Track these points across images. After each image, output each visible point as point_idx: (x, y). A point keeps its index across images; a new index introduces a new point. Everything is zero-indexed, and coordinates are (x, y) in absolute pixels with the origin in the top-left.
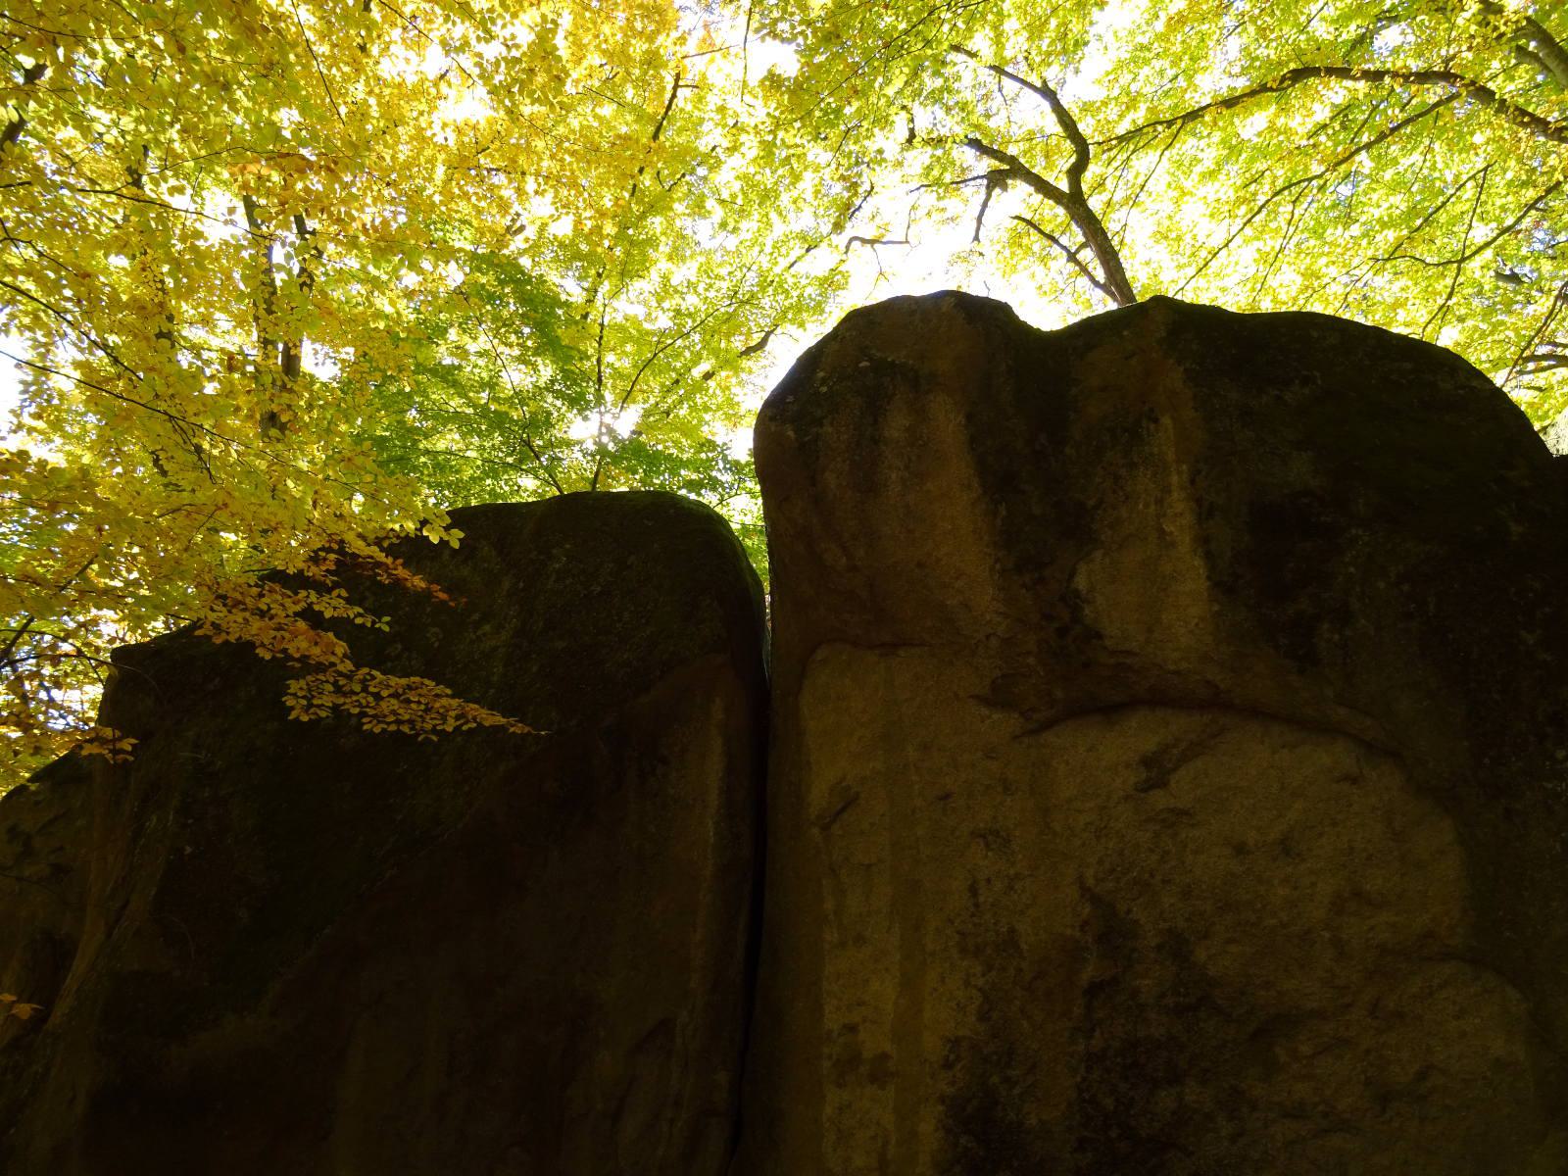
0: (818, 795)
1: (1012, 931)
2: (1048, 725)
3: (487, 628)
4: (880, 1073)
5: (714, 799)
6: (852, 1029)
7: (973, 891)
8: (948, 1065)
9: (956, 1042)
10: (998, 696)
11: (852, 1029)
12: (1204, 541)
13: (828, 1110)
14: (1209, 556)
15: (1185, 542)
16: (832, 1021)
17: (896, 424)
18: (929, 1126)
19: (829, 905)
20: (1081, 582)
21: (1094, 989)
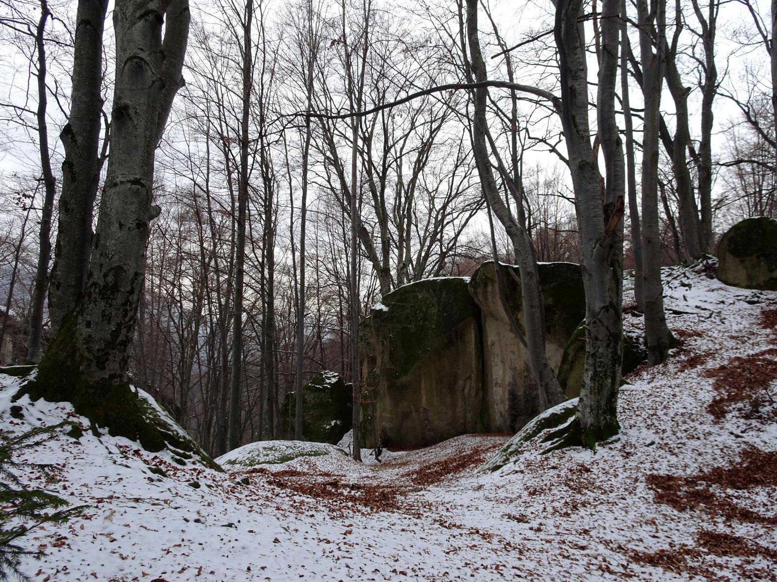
0: (489, 343)
4: (500, 386)
5: (473, 341)
10: (511, 331)
16: (494, 377)
17: (490, 288)
20: (519, 317)
21: (525, 377)
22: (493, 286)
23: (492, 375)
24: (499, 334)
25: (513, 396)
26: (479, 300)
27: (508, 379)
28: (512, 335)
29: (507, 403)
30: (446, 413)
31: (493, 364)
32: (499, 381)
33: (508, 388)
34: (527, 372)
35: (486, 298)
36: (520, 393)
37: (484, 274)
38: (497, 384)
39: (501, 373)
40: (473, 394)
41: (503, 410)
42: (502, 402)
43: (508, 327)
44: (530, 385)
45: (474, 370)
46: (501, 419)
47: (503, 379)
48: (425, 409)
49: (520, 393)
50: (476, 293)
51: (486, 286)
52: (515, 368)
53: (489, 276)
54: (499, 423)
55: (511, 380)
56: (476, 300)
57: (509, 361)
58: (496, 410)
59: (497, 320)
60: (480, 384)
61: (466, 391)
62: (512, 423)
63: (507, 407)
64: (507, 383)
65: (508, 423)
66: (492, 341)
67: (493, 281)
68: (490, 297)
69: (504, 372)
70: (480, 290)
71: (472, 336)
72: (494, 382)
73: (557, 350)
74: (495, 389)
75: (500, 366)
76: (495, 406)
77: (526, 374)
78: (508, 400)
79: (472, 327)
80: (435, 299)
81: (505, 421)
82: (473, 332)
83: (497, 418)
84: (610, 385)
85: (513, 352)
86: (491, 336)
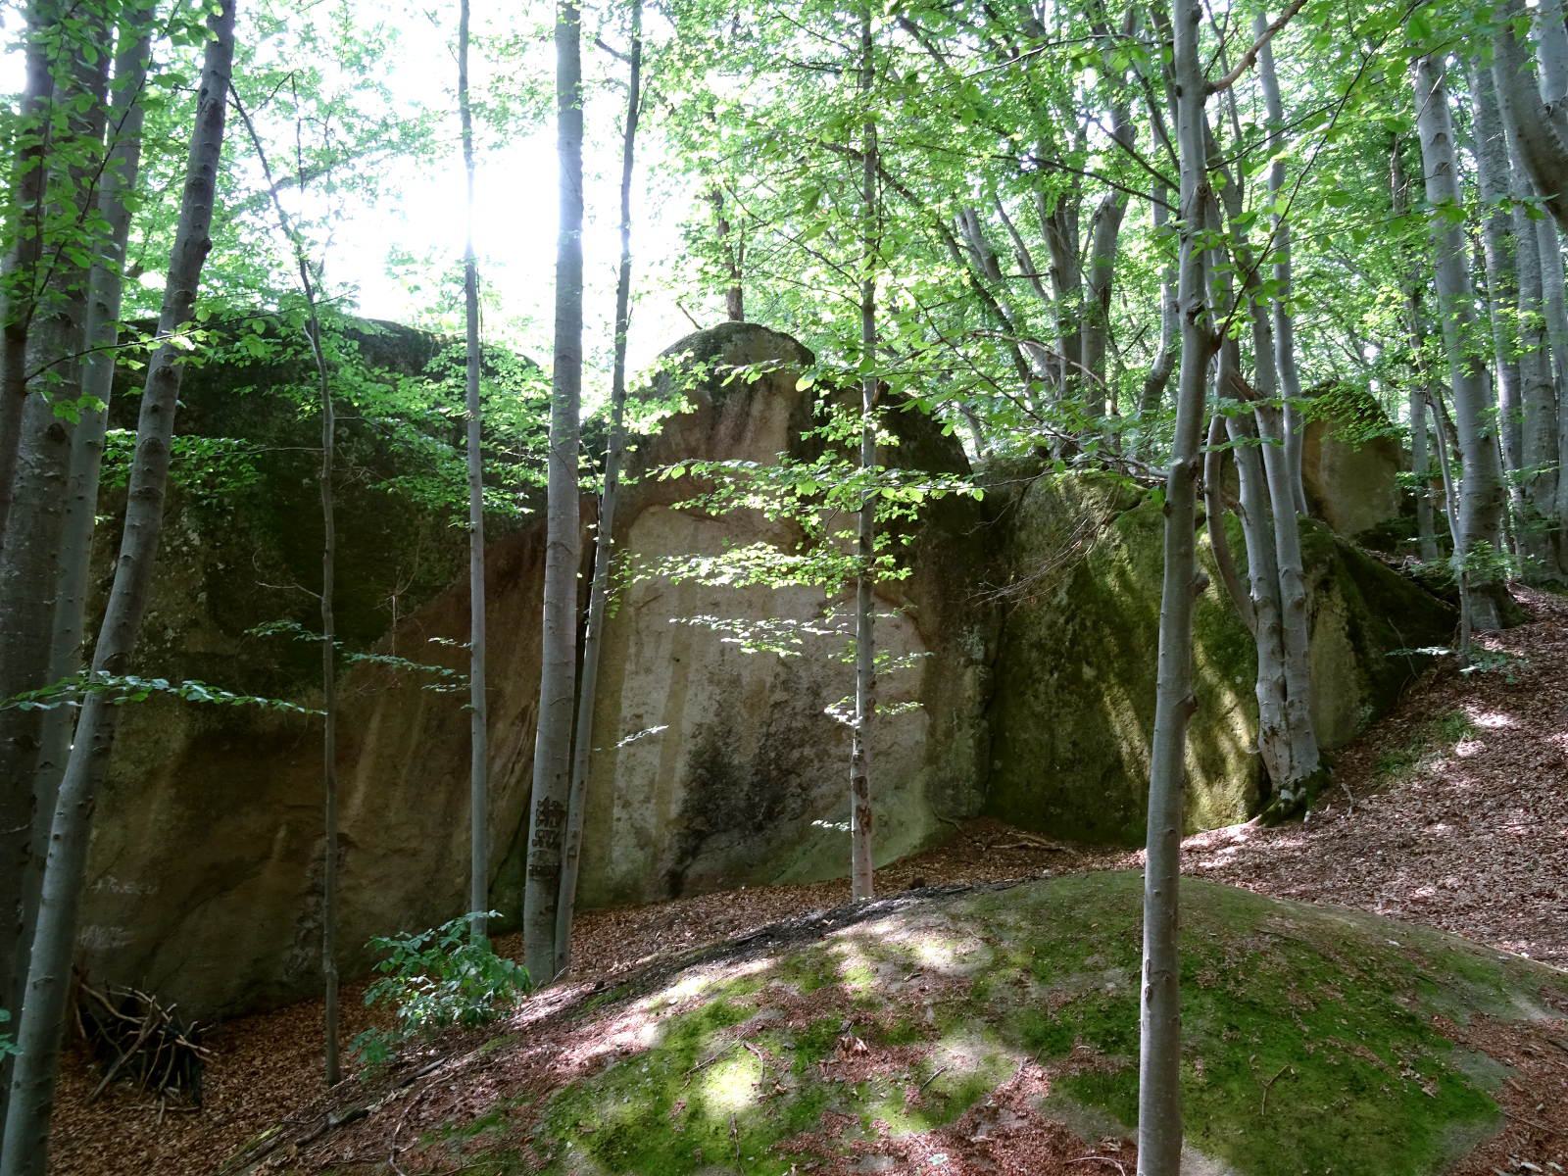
1: (739, 675)
8: (694, 736)
9: (700, 725)
11: (639, 716)
18: (681, 767)
19: (632, 650)
21: (776, 705)
22: (768, 404)
23: (617, 706)
29: (680, 794)
30: (415, 853)
31: (630, 667)
36: (742, 757)
42: (656, 791)
44: (790, 730)
46: (639, 855)
48: (343, 840)
49: (742, 757)
52: (736, 681)
54: (624, 868)
55: (710, 718)
58: (622, 827)
62: (680, 860)
63: (674, 810)
64: (687, 727)
65: (668, 862)
73: (897, 627)
75: (665, 672)
76: (617, 812)
77: (779, 696)
81: (655, 858)
83: (616, 854)
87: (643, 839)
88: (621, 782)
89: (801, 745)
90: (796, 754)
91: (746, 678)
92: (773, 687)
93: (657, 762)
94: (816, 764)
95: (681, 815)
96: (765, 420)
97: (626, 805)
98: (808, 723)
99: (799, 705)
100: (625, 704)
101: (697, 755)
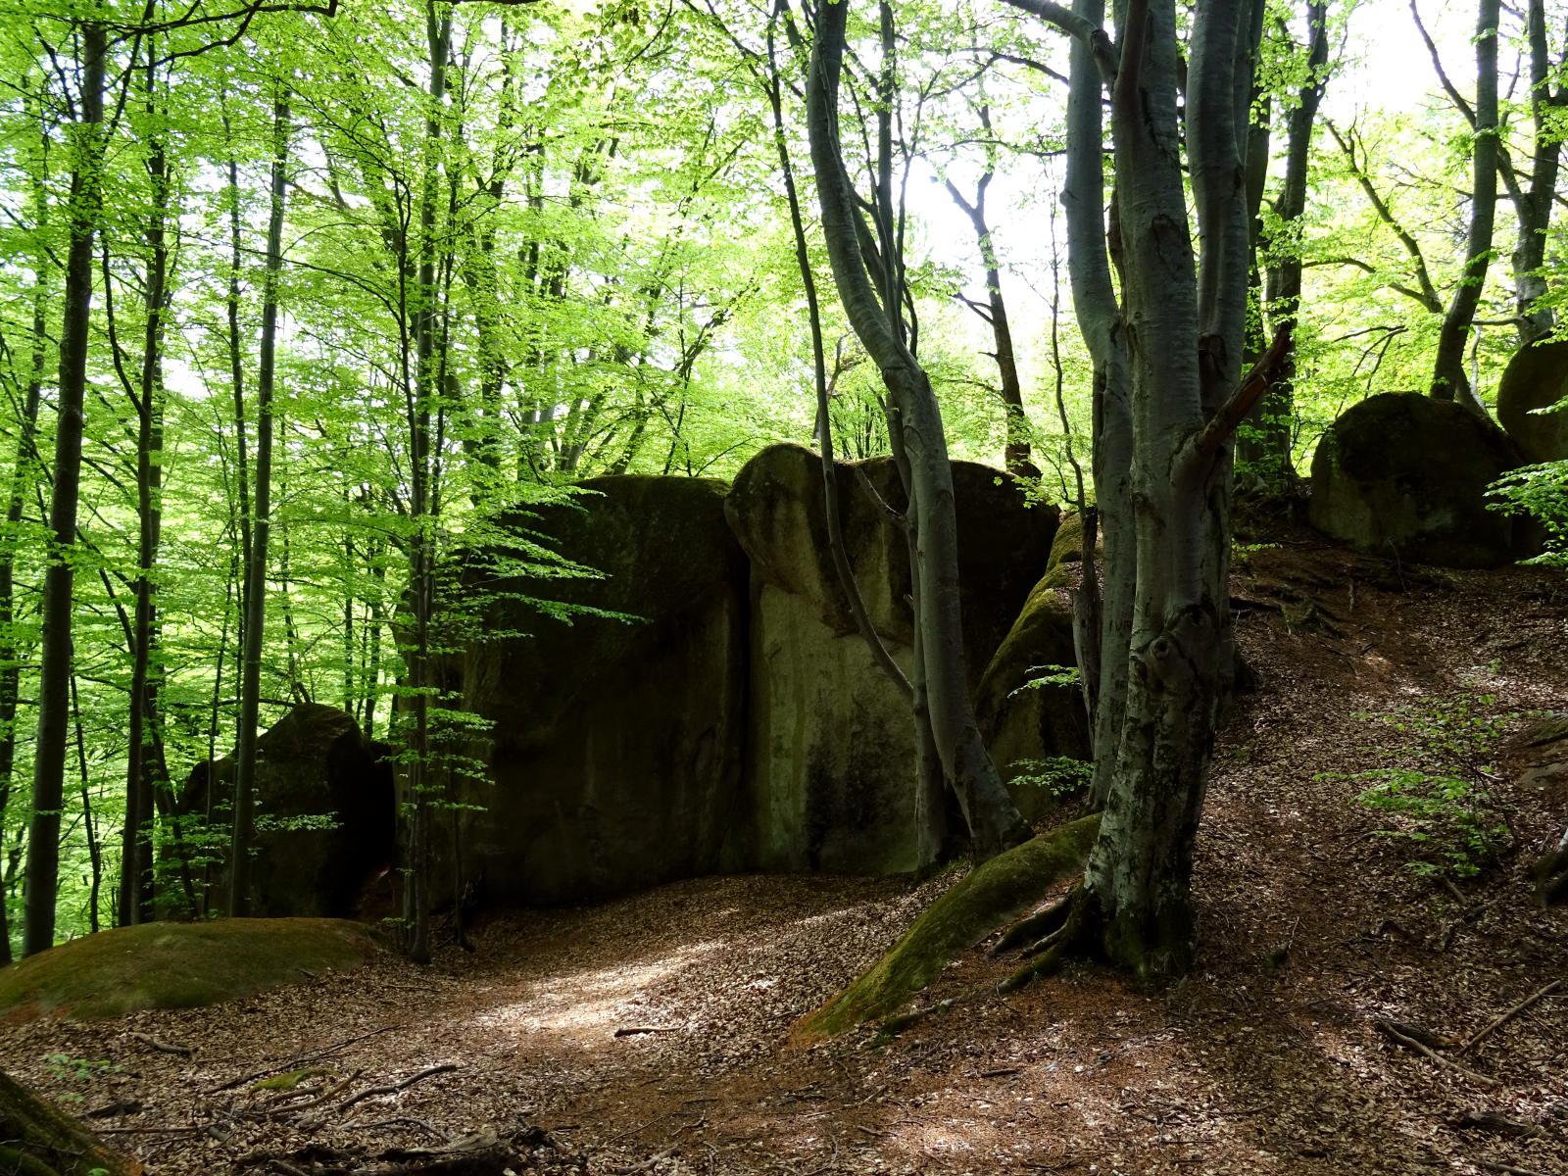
0: (767, 646)
2: (843, 635)
3: (624, 553)
5: (726, 642)
6: (780, 737)
7: (819, 692)
9: (812, 746)
10: (826, 620)
11: (780, 737)
12: (891, 580)
13: (772, 766)
14: (892, 586)
15: (885, 578)
16: (773, 733)
17: (780, 512)
19: (772, 688)
21: (855, 735)
23: (768, 729)
24: (792, 627)
25: (820, 782)
26: (750, 541)
27: (810, 737)
28: (828, 632)
29: (804, 797)
31: (773, 700)
32: (787, 744)
33: (807, 761)
34: (860, 723)
35: (769, 535)
36: (839, 773)
37: (768, 476)
38: (779, 749)
39: (791, 724)
40: (717, 775)
41: (790, 814)
43: (817, 612)
45: (723, 713)
46: (786, 836)
47: (797, 741)
49: (839, 773)
50: (744, 523)
51: (771, 505)
52: (830, 714)
53: (782, 480)
54: (780, 843)
55: (818, 742)
56: (743, 541)
57: (814, 696)
58: (775, 814)
59: (791, 591)
60: (736, 749)
61: (700, 765)
63: (802, 807)
64: (805, 747)
66: (774, 644)
67: (790, 496)
68: (779, 535)
69: (800, 722)
70: (755, 516)
71: (722, 630)
72: (773, 744)
74: (773, 761)
76: (773, 804)
77: (856, 728)
78: (808, 790)
79: (726, 605)
80: (632, 529)
82: (726, 618)
83: (775, 833)
84: (1183, 806)
85: (826, 674)
86: (772, 633)
87: (788, 828)
88: (773, 783)
89: (878, 766)
90: (875, 773)
91: (835, 709)
92: (851, 720)
93: (790, 771)
94: (892, 783)
95: (808, 809)
96: (790, 524)
97: (778, 800)
98: (879, 750)
99: (871, 735)
100: (773, 727)
101: (811, 768)
